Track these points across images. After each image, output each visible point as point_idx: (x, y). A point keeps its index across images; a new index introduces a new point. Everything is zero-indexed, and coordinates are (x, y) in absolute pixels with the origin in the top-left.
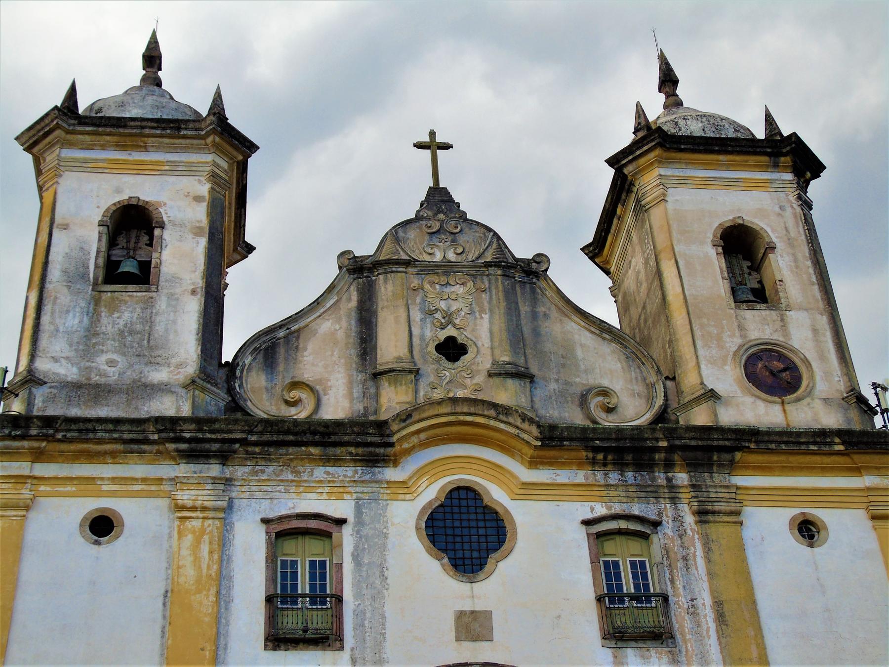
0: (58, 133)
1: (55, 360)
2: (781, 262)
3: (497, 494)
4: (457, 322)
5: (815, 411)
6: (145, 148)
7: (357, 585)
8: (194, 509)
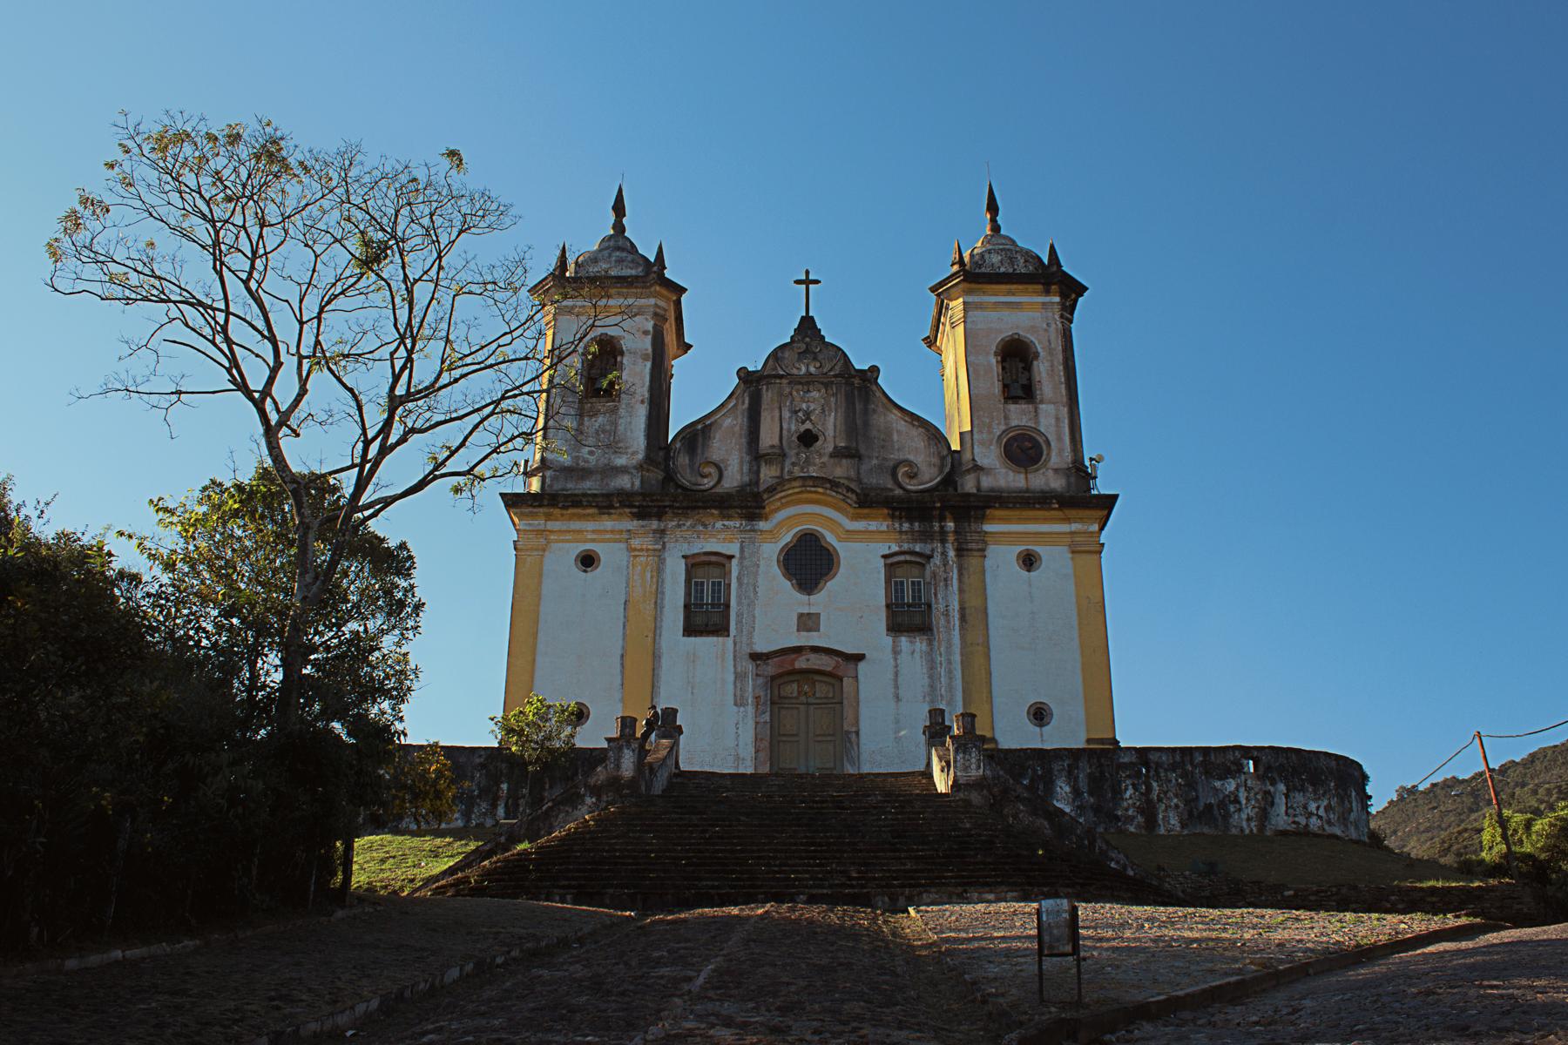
2: (1042, 368)
3: (830, 538)
5: (1047, 479)
7: (739, 597)
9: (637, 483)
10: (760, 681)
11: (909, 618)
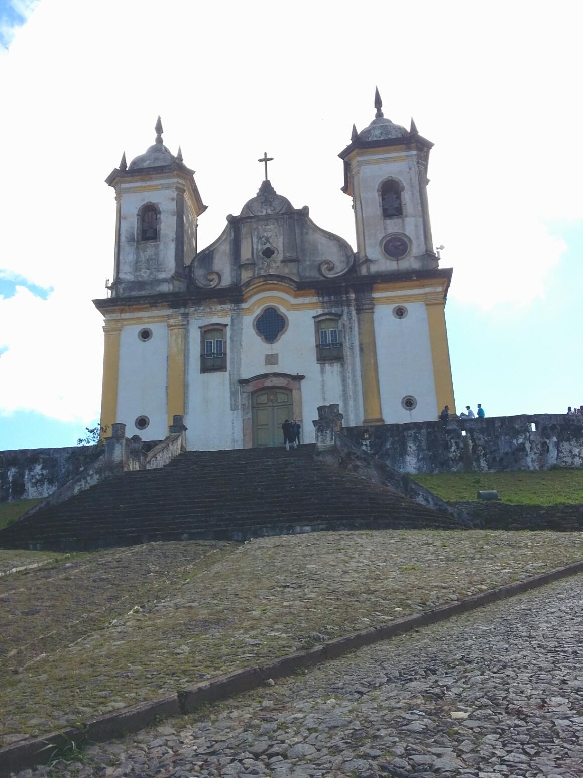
0: (118, 178)
1: (125, 273)
2: (406, 196)
3: (283, 310)
4: (271, 240)
6: (150, 180)
8: (175, 326)
9: (171, 288)
11: (329, 352)
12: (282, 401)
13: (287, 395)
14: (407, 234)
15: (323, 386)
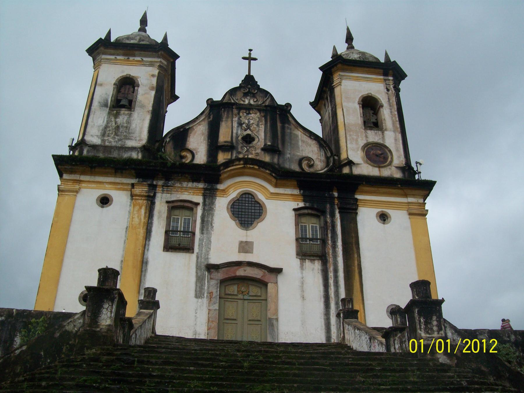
3: (261, 197)
4: (251, 128)
5: (391, 172)
8: (139, 196)
10: (213, 282)
12: (254, 294)
13: (261, 288)
14: (387, 145)
15: (303, 283)
